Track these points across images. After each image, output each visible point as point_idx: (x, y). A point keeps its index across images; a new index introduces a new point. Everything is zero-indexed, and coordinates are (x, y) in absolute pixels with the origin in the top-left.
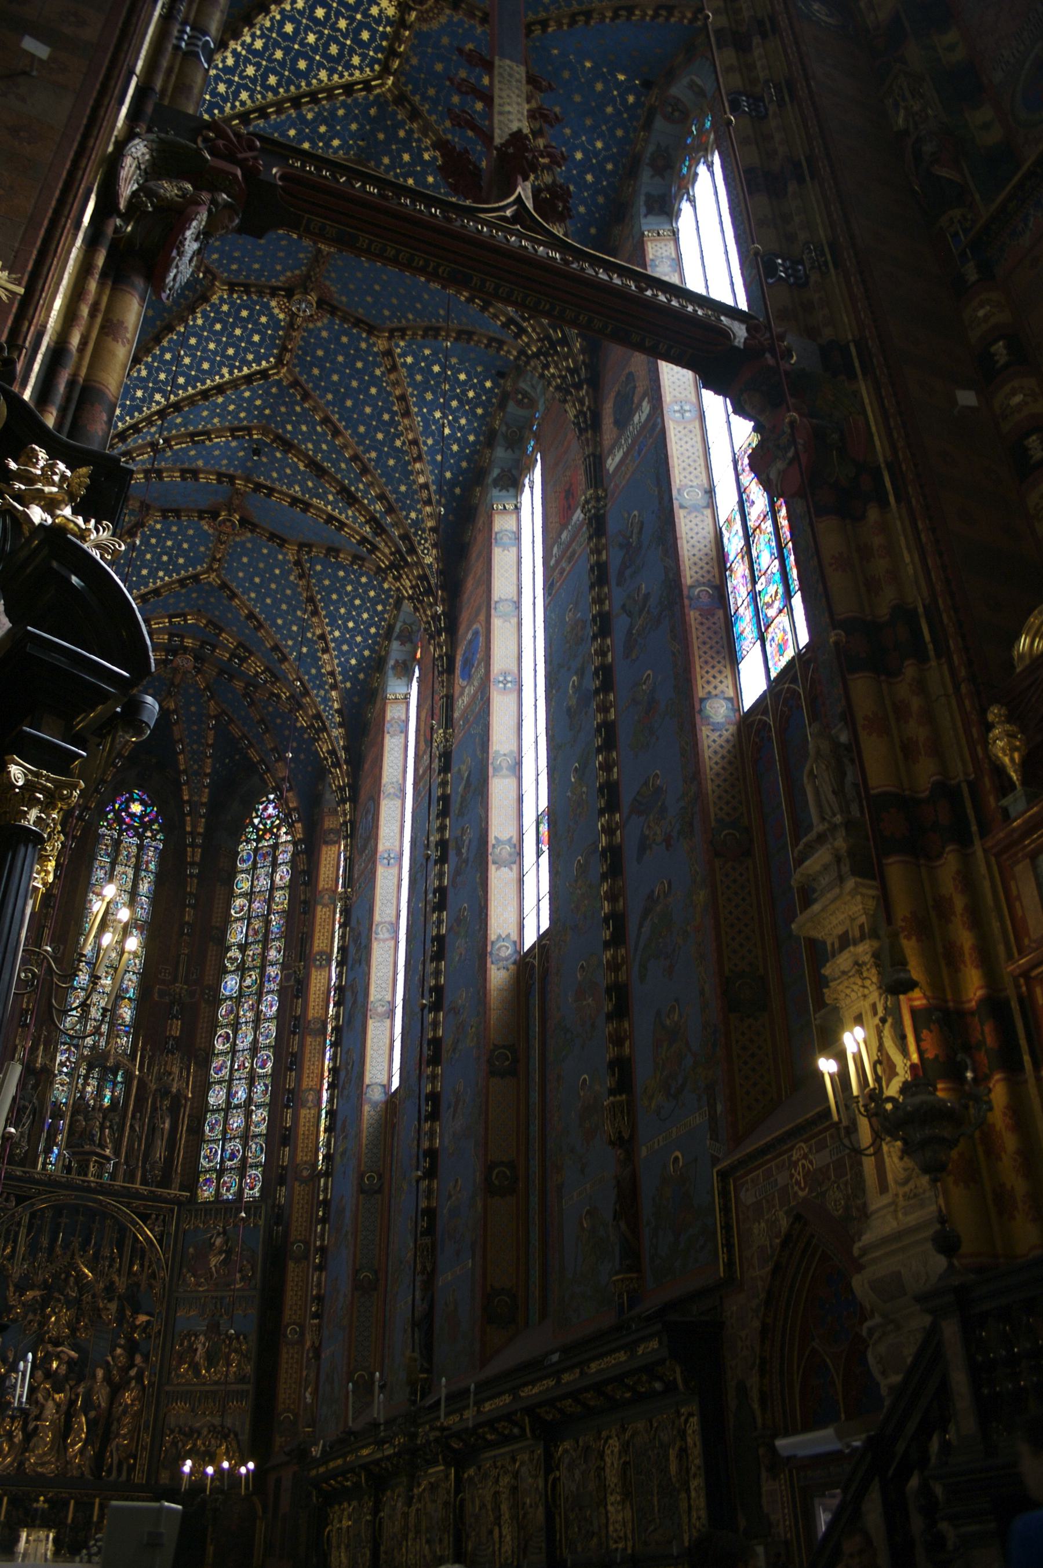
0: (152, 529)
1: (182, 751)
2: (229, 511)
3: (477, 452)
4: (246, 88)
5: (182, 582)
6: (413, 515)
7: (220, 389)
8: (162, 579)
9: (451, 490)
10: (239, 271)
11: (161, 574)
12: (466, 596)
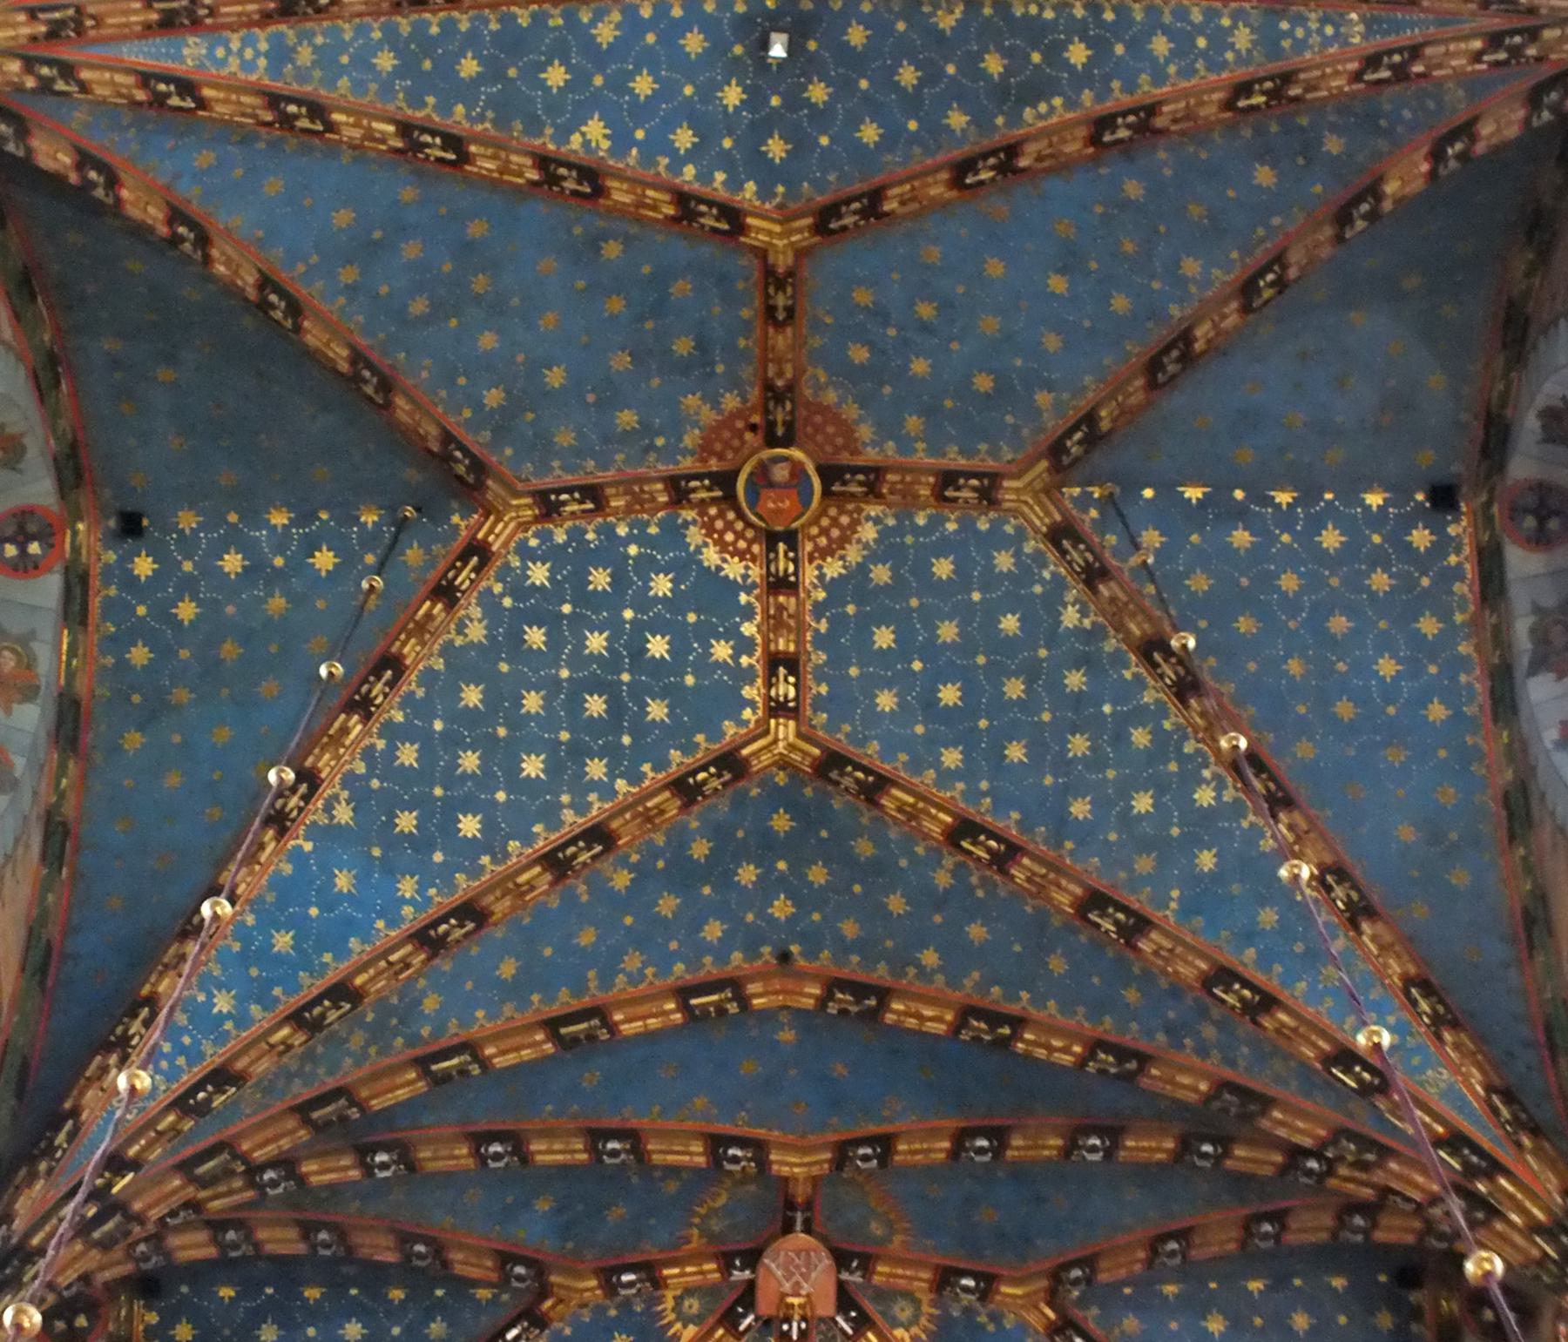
0: (519, 589)
8: (607, 791)
11: (596, 769)
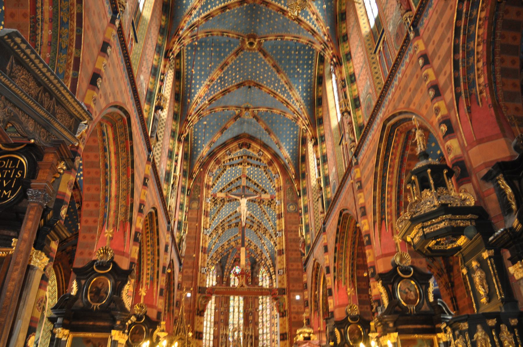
7: (231, 215)
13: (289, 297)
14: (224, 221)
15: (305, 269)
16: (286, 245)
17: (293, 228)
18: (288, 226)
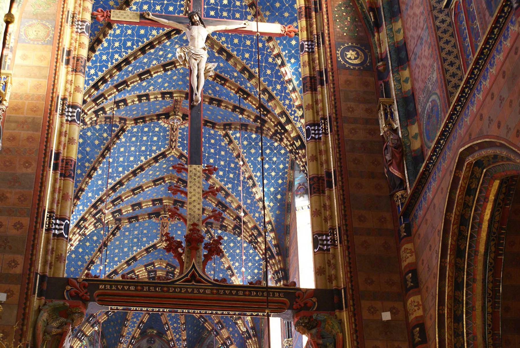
1: (168, 329)
2: (165, 211)
3: (286, 173)
4: (117, 52)
5: (147, 250)
6: (257, 215)
7: (141, 168)
8: (136, 251)
9: (275, 197)
10: (138, 113)
12: (291, 258)
13: (355, 315)
14: (121, 183)
15: (408, 229)
16: (340, 160)
17: (360, 112)
18: (343, 106)
